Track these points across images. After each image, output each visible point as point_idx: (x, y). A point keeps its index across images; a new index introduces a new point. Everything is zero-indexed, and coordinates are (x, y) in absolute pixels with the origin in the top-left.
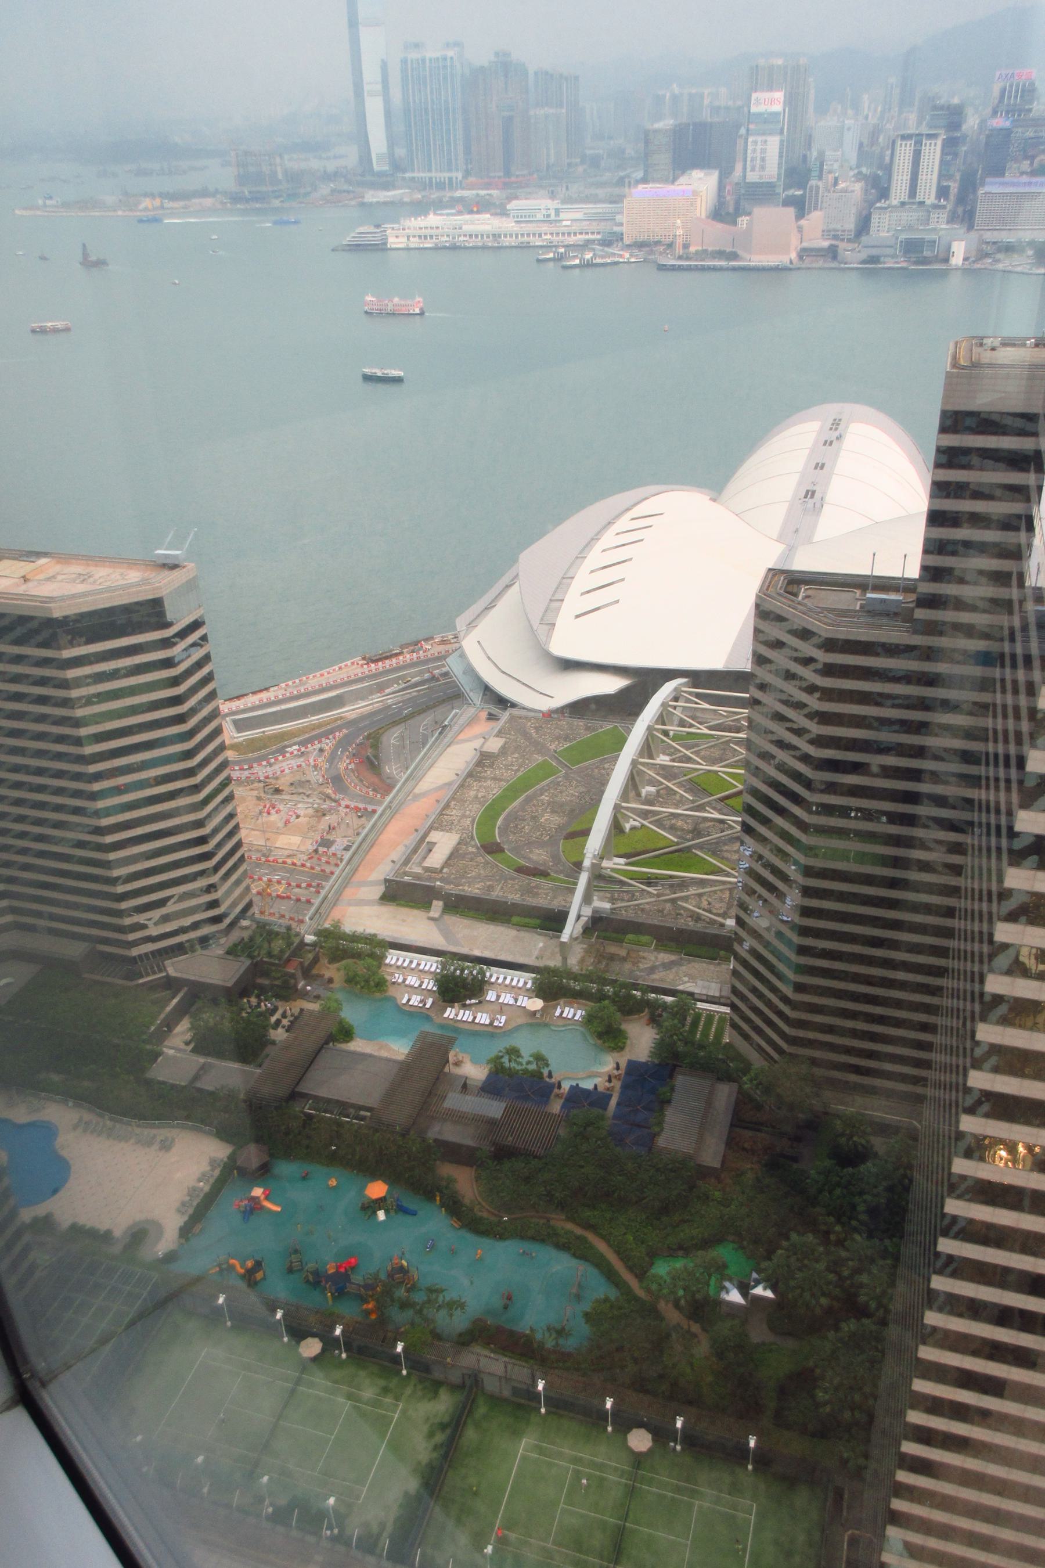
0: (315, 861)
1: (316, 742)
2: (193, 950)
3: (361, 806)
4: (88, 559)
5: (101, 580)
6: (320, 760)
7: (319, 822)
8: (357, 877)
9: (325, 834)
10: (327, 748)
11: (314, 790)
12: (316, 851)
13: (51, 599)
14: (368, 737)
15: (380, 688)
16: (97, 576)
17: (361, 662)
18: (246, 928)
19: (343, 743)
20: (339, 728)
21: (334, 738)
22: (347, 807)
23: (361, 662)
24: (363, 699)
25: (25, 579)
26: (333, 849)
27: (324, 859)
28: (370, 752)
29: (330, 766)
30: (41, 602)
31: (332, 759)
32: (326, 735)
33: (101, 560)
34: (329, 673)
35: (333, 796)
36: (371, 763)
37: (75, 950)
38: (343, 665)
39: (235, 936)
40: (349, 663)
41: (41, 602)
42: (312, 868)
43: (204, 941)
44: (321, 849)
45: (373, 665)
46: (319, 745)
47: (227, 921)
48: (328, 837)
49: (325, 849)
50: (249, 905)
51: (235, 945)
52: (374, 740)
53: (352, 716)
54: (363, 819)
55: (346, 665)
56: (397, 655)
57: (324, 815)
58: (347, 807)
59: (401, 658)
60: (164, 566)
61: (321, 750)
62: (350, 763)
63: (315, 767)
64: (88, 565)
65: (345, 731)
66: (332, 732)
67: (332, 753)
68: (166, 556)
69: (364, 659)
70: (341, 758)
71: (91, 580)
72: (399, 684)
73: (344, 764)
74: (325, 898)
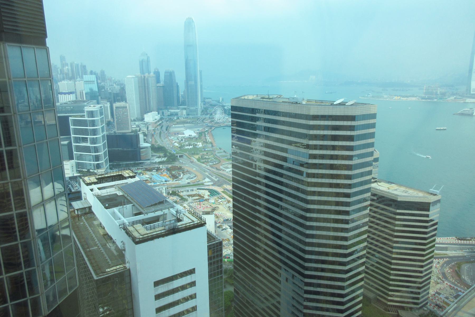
0: (433, 297)
1: (437, 259)
2: (407, 310)
3: (453, 286)
4: (407, 187)
5: (411, 194)
6: (438, 265)
7: (436, 285)
8: (462, 309)
9: (438, 290)
10: (440, 262)
11: (435, 274)
12: (435, 295)
13: (398, 195)
14: (456, 264)
15: (461, 249)
16: (409, 192)
17: (455, 239)
18: (425, 310)
19: (447, 263)
20: (446, 258)
21: (444, 260)
22: (447, 284)
23: (455, 239)
24: (455, 251)
25: (389, 189)
26: (441, 296)
27: (437, 298)
28: (457, 269)
29: (441, 268)
30: (395, 195)
31: (442, 266)
32: (441, 258)
33: (411, 188)
34: (443, 239)
35: (442, 279)
36: (457, 273)
37: (371, 295)
38: (448, 238)
39: (421, 311)
40: (451, 238)
41: (395, 195)
42: (432, 299)
43: (411, 309)
44: (436, 295)
45: (460, 241)
46: (438, 261)
47: (420, 305)
48: (439, 292)
49: (438, 295)
50: (427, 303)
51: (422, 314)
52: (459, 266)
53: (451, 255)
54: (452, 290)
55: (450, 238)
56: (469, 240)
57: (438, 284)
58: (447, 284)
59: (471, 241)
60: (431, 194)
61: (439, 262)
62: (449, 270)
63: (436, 267)
64: (406, 189)
65: (448, 259)
66: (443, 258)
67: (443, 264)
68: (433, 191)
69: (456, 238)
70: (446, 267)
71: (408, 193)
72: (469, 250)
73: (447, 270)
74: (447, 312)
